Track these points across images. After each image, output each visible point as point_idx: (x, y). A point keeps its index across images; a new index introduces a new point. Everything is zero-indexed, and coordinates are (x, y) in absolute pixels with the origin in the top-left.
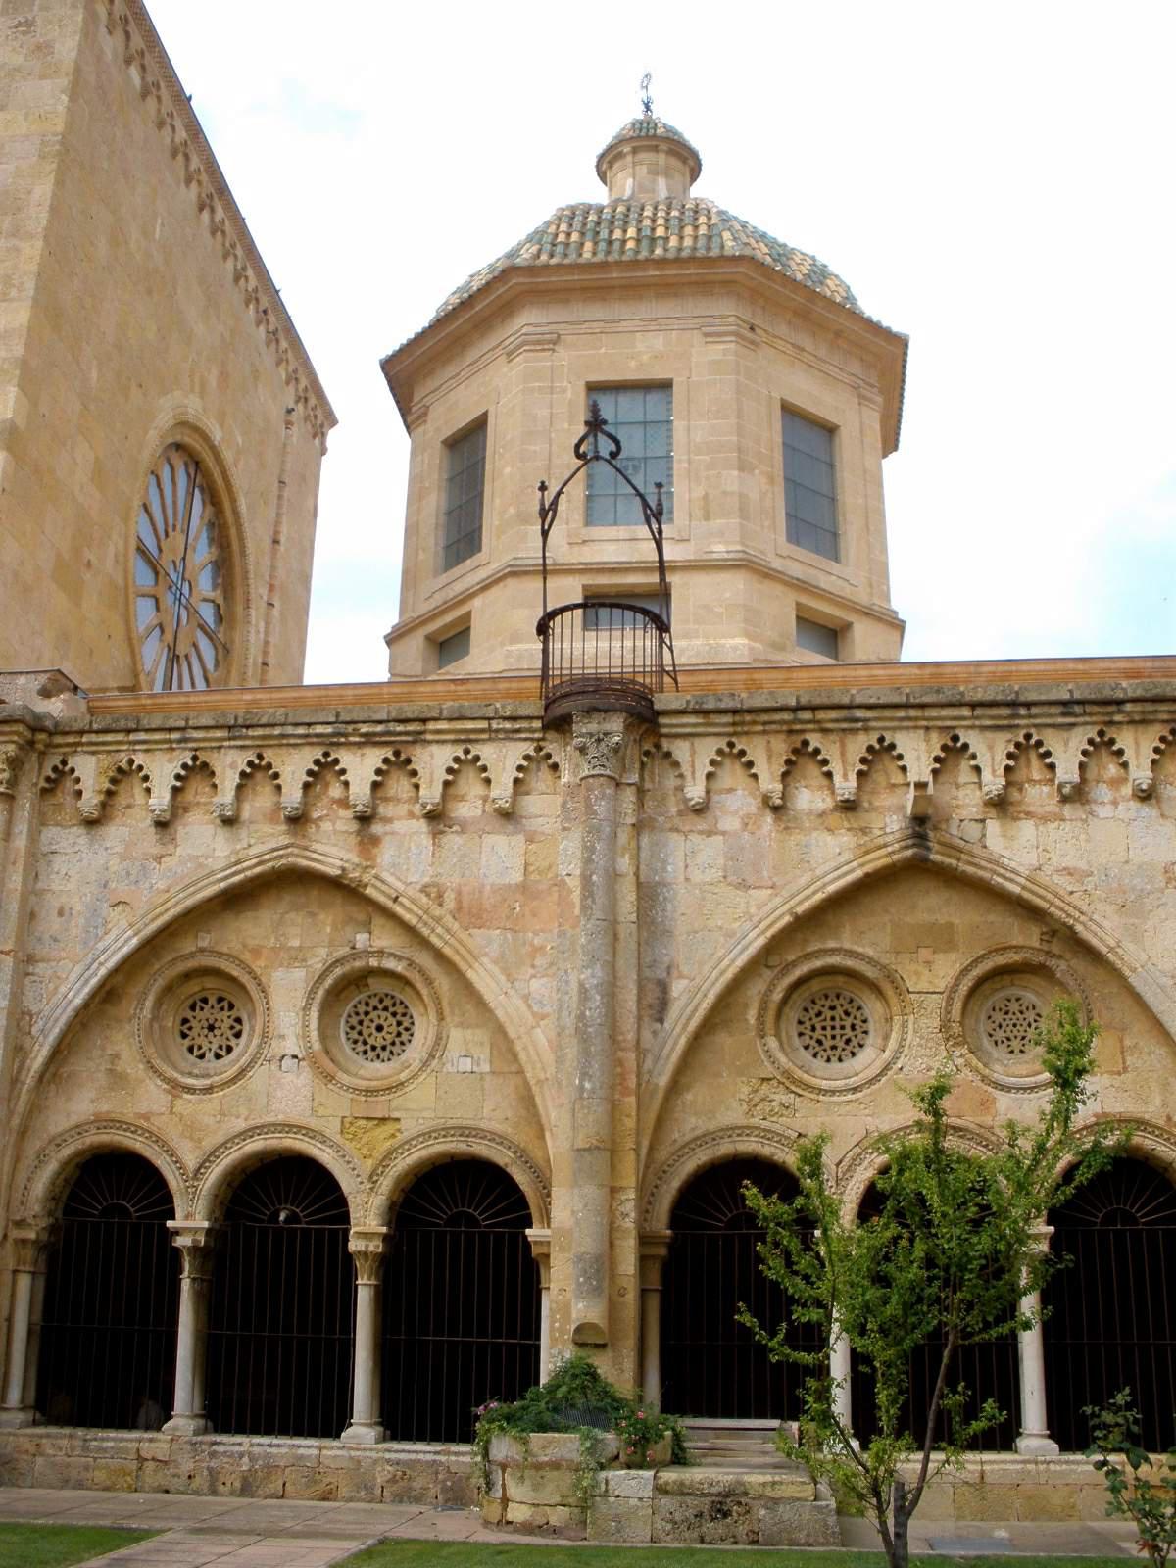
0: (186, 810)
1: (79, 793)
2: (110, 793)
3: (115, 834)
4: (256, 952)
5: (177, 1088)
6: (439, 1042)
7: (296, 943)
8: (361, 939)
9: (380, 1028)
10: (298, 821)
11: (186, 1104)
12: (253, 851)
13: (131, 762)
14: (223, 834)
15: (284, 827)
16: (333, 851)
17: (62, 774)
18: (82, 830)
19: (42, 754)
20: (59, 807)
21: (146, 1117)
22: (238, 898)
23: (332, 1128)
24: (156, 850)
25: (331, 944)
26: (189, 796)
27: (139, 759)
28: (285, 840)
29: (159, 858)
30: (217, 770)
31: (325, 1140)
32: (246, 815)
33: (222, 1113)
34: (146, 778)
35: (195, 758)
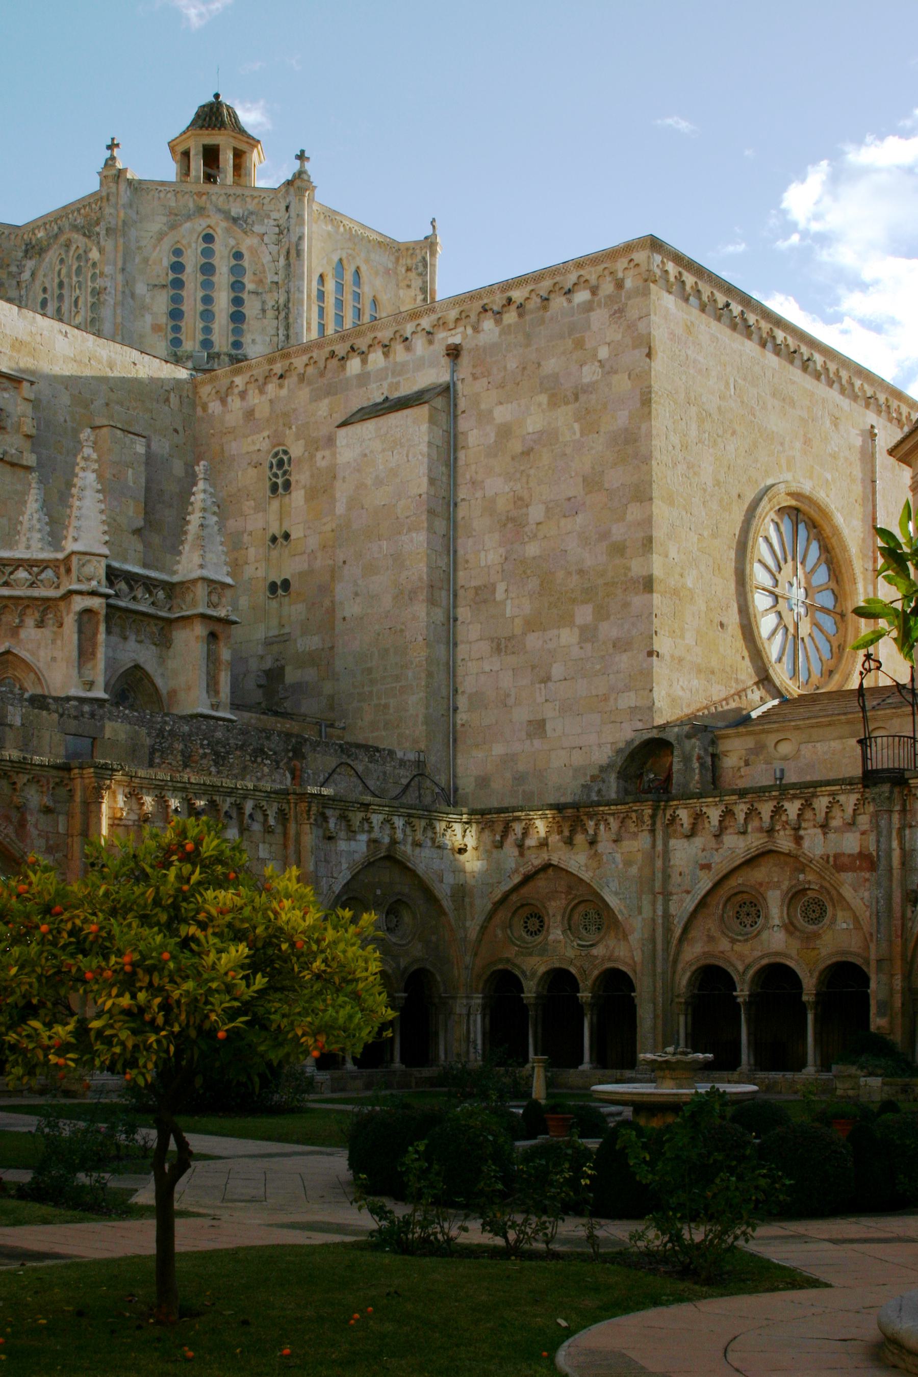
0: (726, 828)
1: (682, 825)
2: (694, 824)
3: (698, 841)
4: (761, 884)
5: (733, 941)
6: (834, 916)
7: (776, 880)
8: (801, 877)
9: (814, 911)
10: (771, 831)
11: (738, 947)
12: (754, 845)
13: (701, 811)
14: (742, 837)
15: (765, 834)
16: (785, 843)
17: (674, 819)
18: (685, 840)
19: (664, 810)
20: (675, 831)
21: (722, 952)
22: (751, 862)
23: (794, 953)
24: (715, 846)
25: (790, 879)
26: (726, 823)
27: (704, 809)
28: (766, 840)
29: (717, 850)
30: (736, 812)
31: (791, 958)
32: (749, 830)
33: (752, 950)
34: (708, 817)
35: (726, 808)
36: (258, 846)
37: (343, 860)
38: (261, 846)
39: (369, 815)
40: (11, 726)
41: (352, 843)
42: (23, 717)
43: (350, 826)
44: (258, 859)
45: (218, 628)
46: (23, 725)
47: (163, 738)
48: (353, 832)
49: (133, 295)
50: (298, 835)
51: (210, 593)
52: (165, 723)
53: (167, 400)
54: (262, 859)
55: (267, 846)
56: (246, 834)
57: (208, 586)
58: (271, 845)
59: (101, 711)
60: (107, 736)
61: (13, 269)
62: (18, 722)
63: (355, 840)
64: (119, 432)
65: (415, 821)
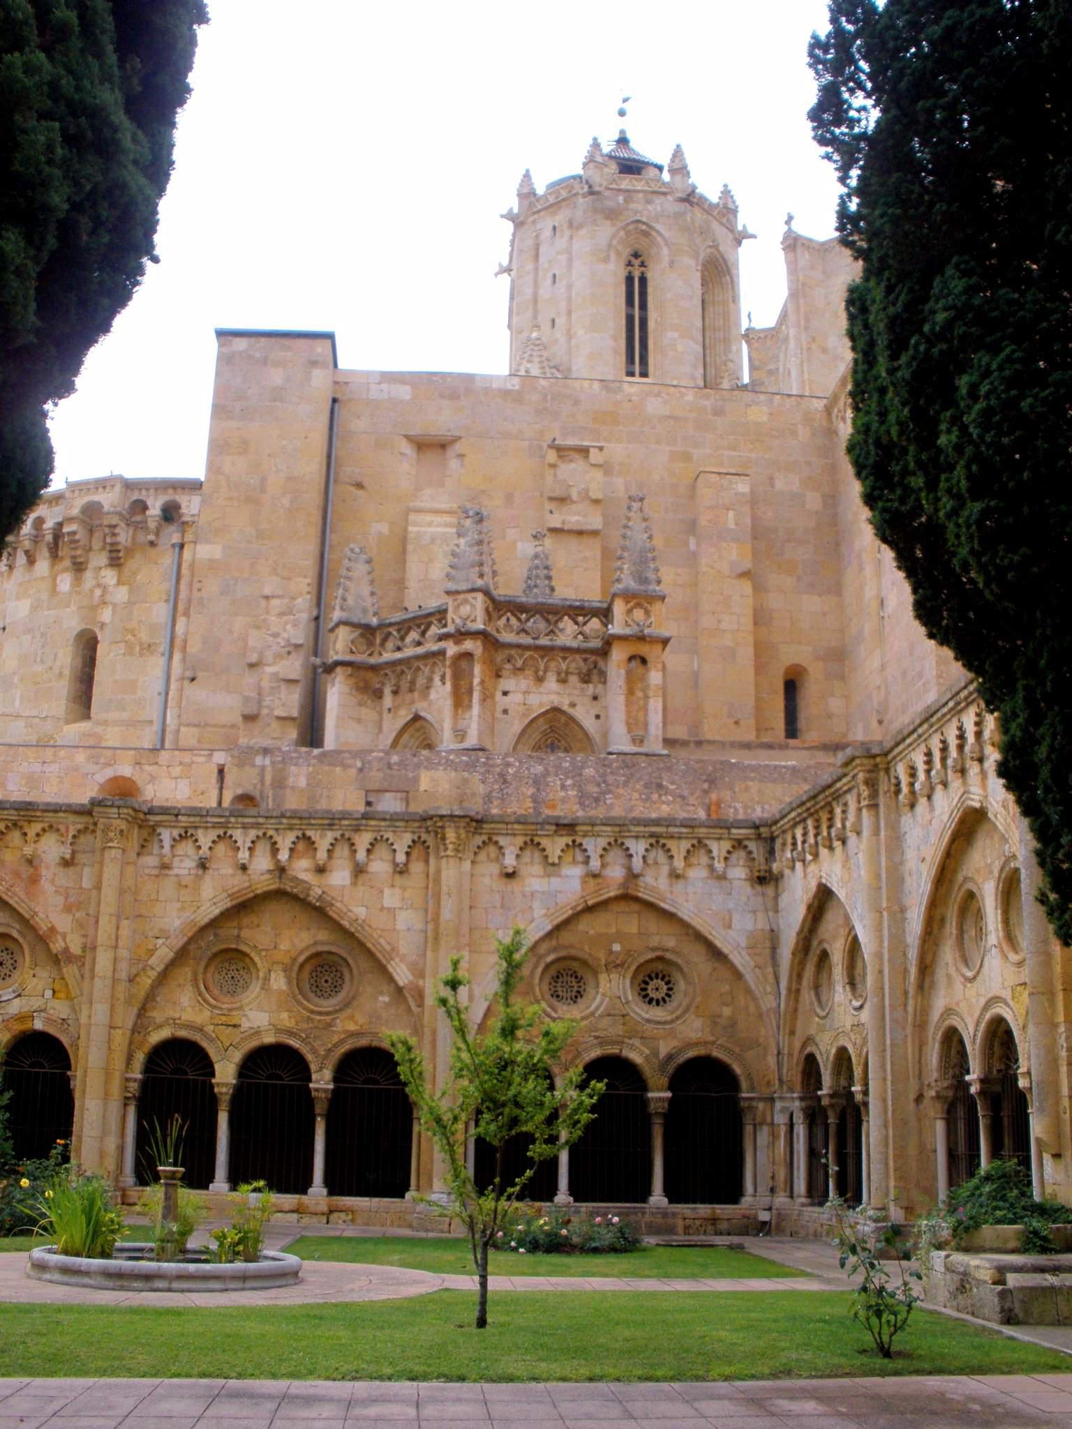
36: (382, 892)
37: (536, 905)
38: (387, 891)
39: (579, 840)
40: (293, 788)
41: (553, 880)
42: (310, 777)
43: (546, 857)
44: (382, 908)
45: (644, 649)
46: (308, 785)
47: (505, 781)
48: (553, 864)
49: (824, 350)
50: (438, 872)
51: (629, 611)
52: (508, 765)
53: (794, 433)
54: (389, 909)
55: (397, 891)
56: (362, 878)
57: (627, 602)
58: (404, 889)
59: (415, 760)
60: (422, 788)
61: (772, 367)
62: (303, 782)
63: (560, 876)
64: (713, 476)
65: (671, 844)
